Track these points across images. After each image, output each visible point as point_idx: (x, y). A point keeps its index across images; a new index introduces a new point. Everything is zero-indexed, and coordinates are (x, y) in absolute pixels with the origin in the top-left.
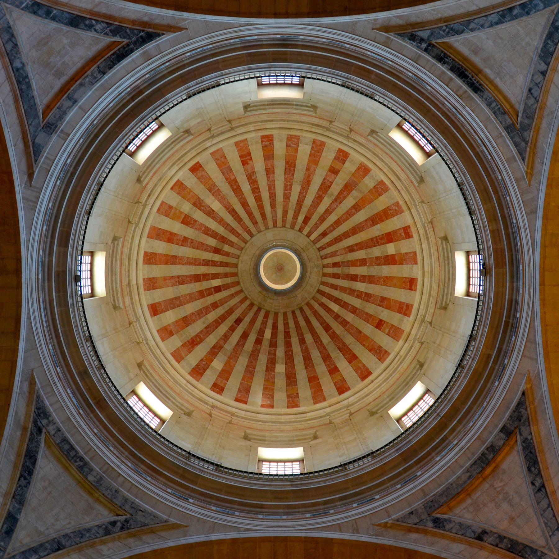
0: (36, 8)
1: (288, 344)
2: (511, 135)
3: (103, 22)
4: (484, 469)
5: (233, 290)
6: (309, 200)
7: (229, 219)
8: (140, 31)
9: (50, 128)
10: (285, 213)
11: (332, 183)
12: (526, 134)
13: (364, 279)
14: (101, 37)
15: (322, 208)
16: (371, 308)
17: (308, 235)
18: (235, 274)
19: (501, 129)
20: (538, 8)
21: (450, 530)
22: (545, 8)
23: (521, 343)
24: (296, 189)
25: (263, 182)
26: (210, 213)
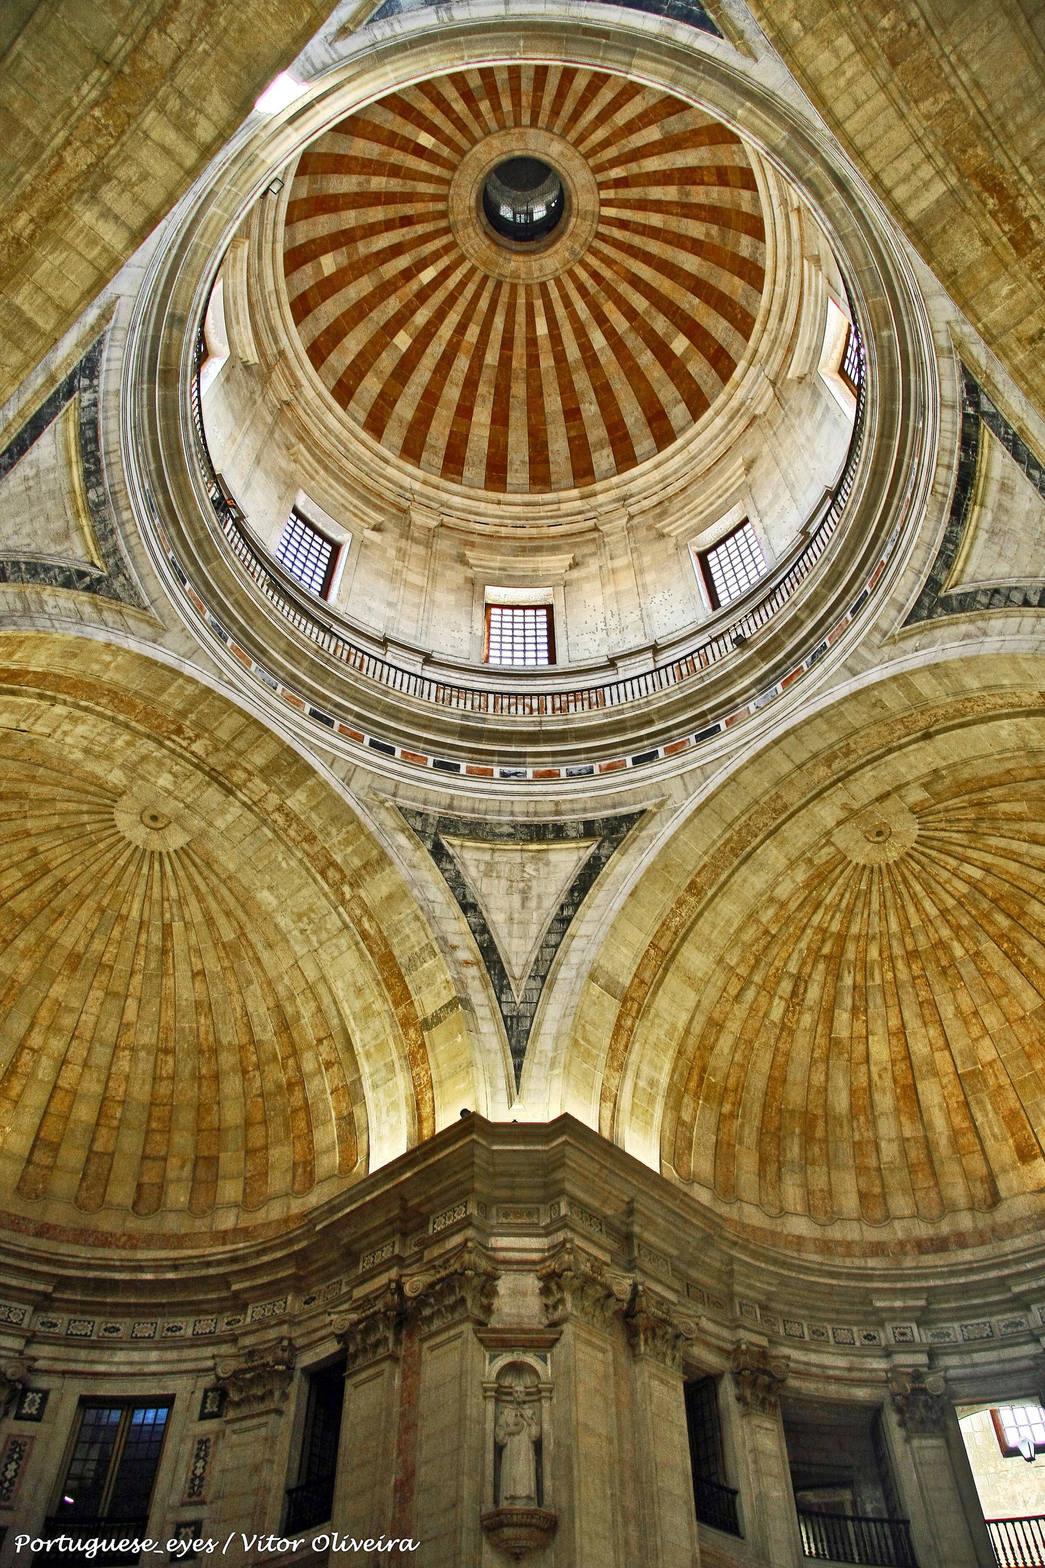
1: (440, 315)
4: (531, 841)
5: (437, 171)
6: (652, 164)
10: (606, 144)
11: (702, 183)
13: (610, 334)
15: (656, 193)
16: (582, 381)
17: (605, 203)
18: (461, 153)
19: (927, 571)
21: (443, 871)
23: (695, 761)
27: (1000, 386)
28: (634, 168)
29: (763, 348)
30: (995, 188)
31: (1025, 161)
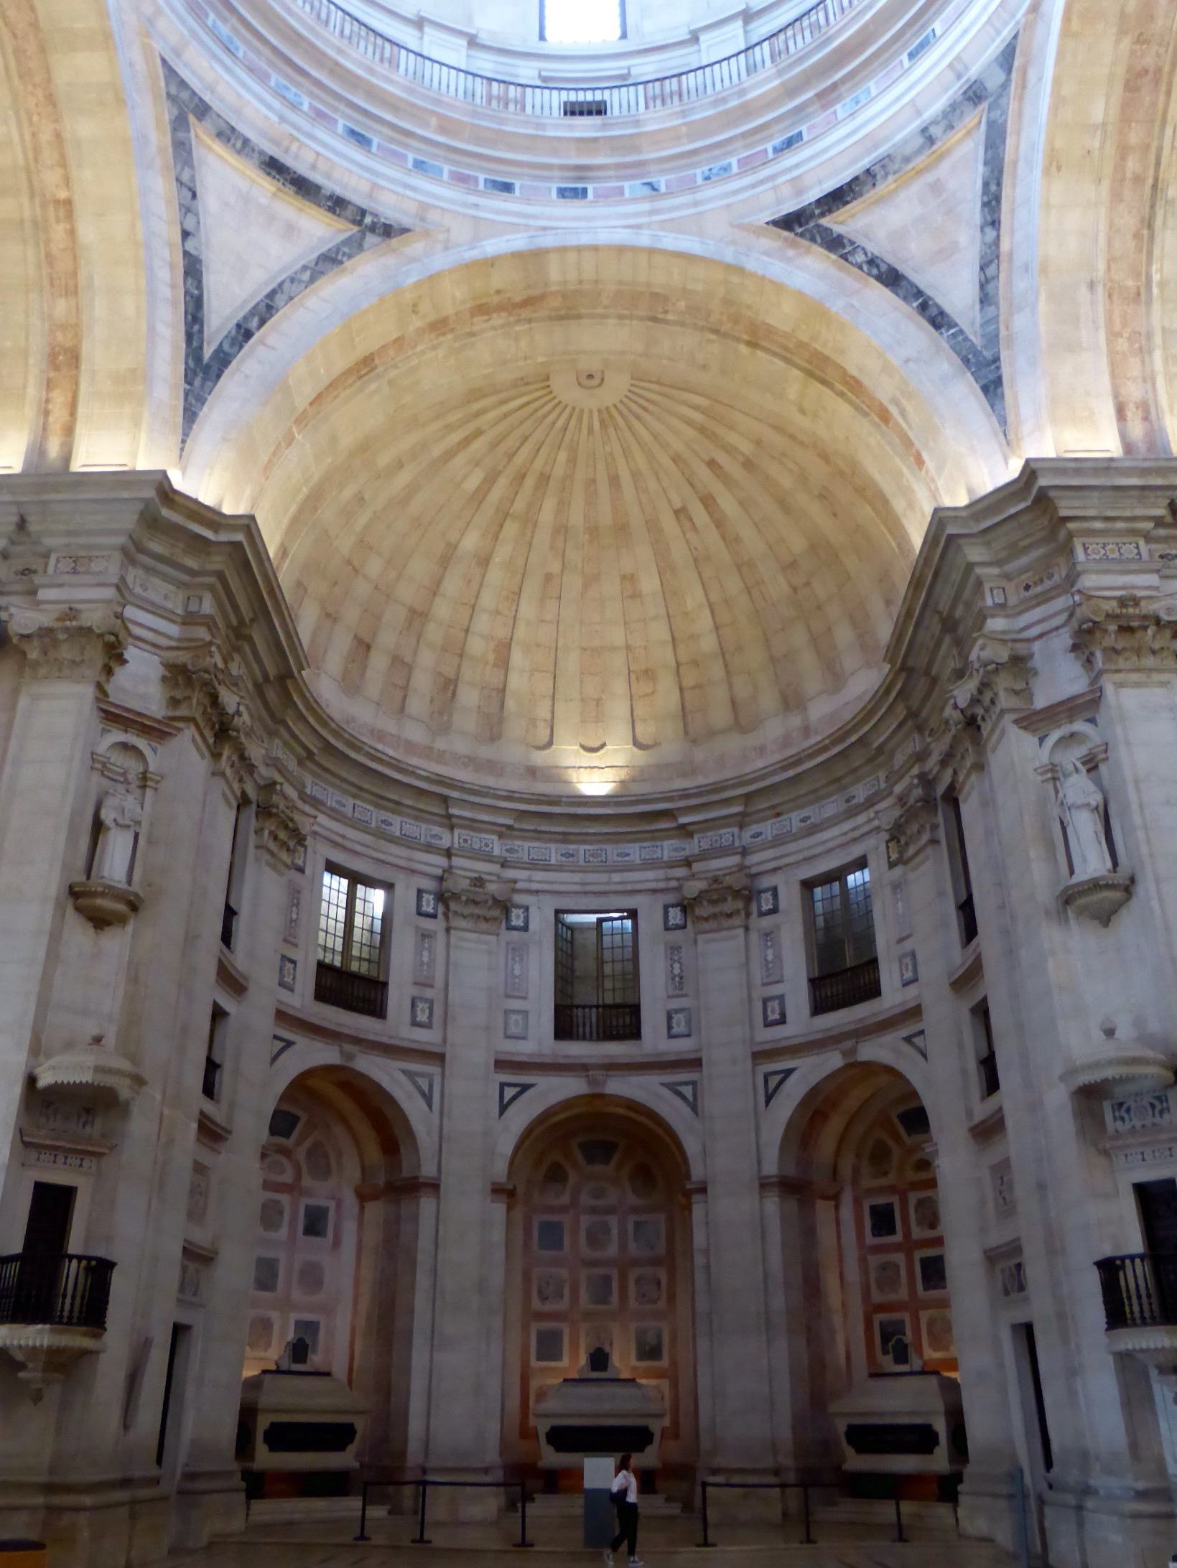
2: (196, 100)
3: (851, 263)
8: (802, 235)
12: (175, 112)
14: (861, 241)
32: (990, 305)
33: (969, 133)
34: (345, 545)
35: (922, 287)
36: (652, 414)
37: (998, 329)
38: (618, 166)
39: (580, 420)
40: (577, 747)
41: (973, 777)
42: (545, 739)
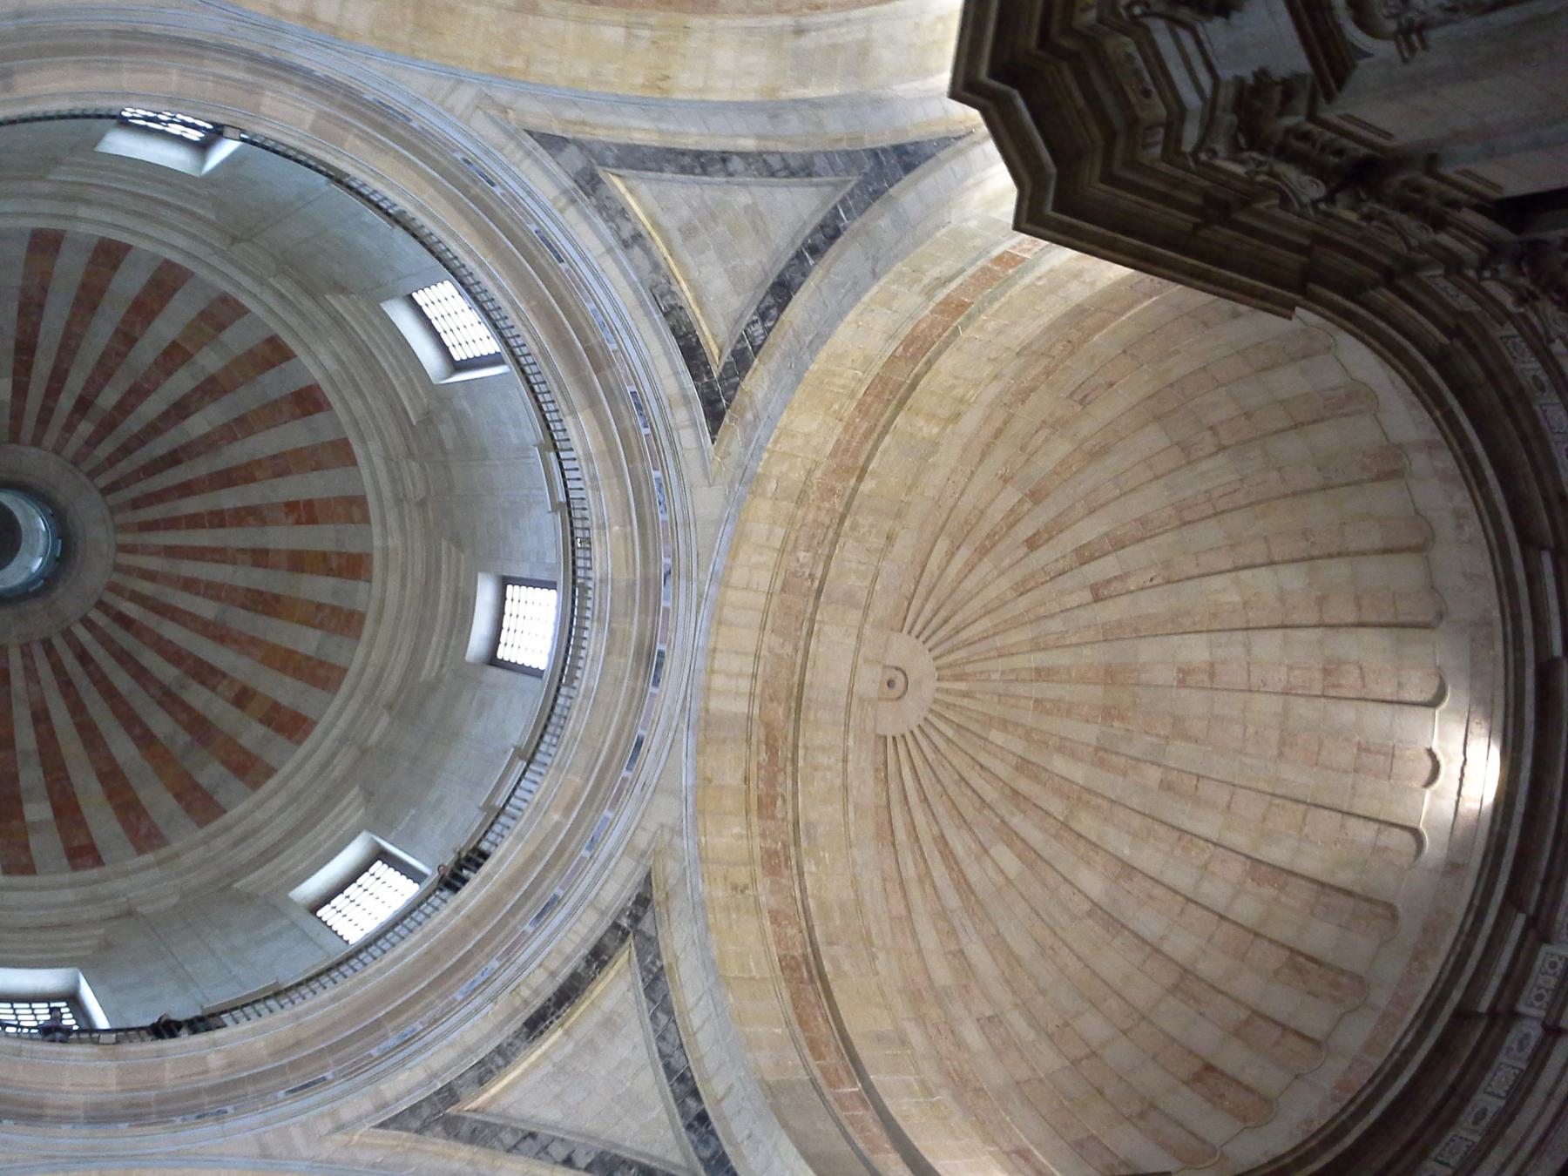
0: (829, 231)
2: (436, 1099)
7: (159, 447)
8: (729, 400)
9: (589, 183)
11: (213, 689)
12: (439, 1129)
19: (449, 1077)
20: (701, 1147)
22: (701, 1159)
24: (206, 609)
25: (233, 538)
26: (180, 410)
27: (674, 915)
28: (152, 621)
29: (187, 859)
30: (772, 750)
31: (805, 747)
32: (813, 164)
33: (631, 191)
34: (1049, 1060)
35: (792, 252)
36: (954, 613)
37: (839, 153)
38: (644, 610)
39: (948, 706)
40: (1428, 793)
41: (1448, 171)
42: (1407, 836)
